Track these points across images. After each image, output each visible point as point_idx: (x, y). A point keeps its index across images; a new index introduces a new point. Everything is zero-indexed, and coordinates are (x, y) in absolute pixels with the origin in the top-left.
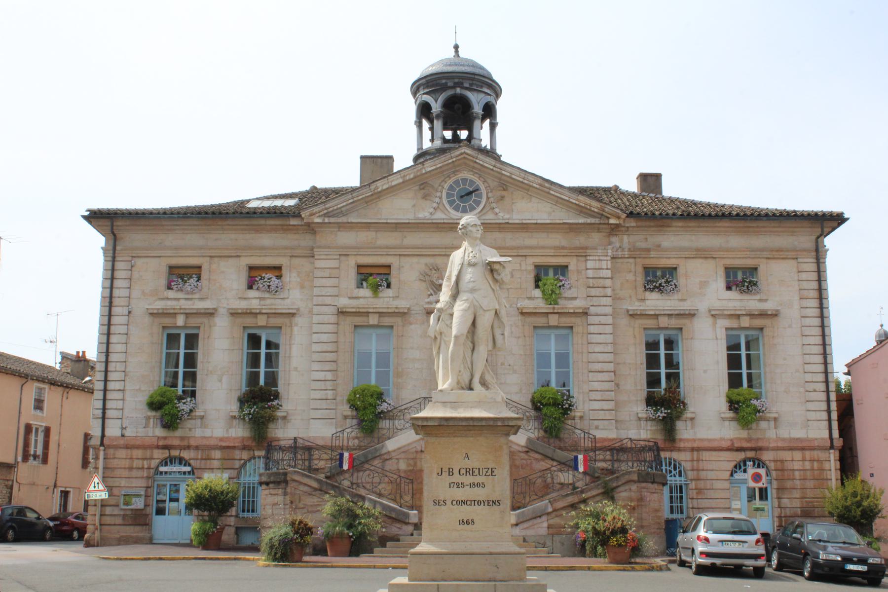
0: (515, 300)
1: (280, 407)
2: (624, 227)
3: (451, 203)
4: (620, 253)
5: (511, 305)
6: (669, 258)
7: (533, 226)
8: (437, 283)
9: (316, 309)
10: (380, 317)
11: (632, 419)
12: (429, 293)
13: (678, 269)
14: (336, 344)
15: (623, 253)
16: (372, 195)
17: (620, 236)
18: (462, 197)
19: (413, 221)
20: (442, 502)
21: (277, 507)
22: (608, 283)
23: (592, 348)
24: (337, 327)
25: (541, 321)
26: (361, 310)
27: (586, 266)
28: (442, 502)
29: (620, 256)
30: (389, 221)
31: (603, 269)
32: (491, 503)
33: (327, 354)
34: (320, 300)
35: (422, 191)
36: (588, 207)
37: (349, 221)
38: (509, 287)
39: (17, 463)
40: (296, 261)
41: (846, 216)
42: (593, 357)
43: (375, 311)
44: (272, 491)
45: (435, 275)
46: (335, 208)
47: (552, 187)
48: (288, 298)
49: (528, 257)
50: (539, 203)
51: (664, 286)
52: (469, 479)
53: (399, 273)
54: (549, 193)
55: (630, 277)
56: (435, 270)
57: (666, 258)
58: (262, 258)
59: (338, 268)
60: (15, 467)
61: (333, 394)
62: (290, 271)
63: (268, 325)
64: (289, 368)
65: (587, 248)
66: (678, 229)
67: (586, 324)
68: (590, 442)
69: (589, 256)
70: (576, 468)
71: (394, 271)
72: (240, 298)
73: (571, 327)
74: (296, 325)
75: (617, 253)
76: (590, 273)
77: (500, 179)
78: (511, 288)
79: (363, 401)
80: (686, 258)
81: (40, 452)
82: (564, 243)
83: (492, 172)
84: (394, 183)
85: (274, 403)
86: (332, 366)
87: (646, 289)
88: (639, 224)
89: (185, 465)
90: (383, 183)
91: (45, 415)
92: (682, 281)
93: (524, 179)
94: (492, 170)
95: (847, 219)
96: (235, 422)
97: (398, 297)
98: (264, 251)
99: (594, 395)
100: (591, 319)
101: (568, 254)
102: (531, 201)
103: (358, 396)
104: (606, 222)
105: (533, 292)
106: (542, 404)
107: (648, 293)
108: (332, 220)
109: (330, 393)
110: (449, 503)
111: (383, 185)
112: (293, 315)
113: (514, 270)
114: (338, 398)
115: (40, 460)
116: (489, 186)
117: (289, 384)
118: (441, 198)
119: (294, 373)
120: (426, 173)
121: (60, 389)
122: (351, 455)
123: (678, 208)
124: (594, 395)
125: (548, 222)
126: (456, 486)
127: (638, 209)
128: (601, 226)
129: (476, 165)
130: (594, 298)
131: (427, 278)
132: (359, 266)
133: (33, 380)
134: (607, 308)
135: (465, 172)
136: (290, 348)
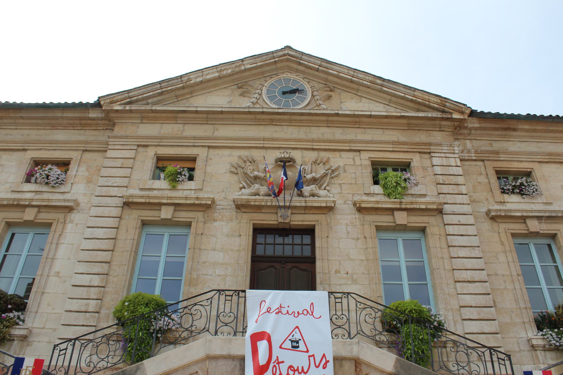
0: (350, 196)
1: (21, 323)
2: (466, 128)
3: (271, 98)
4: (466, 155)
5: (345, 201)
6: (521, 161)
8: (252, 175)
9: (96, 201)
10: (175, 210)
11: (522, 348)
12: (241, 185)
13: (533, 173)
14: (113, 241)
15: (470, 155)
16: (183, 88)
17: (462, 140)
18: (284, 93)
19: (227, 110)
22: (461, 180)
23: (454, 252)
24: (119, 222)
25: (385, 220)
26: (152, 201)
27: (432, 163)
29: (467, 158)
30: (198, 109)
31: (453, 166)
33: (99, 252)
34: (104, 191)
35: (240, 91)
36: (427, 103)
37: (154, 108)
38: (342, 182)
40: (87, 155)
42: (458, 263)
43: (169, 201)
45: (249, 168)
46: (140, 97)
47: (385, 83)
48: (69, 192)
49: (361, 152)
50: (370, 103)
51: (525, 186)
53: (206, 165)
54: (381, 91)
55: (482, 179)
56: (250, 162)
57: (518, 161)
58: (51, 152)
59: (134, 158)
61: (97, 305)
62: (79, 165)
63: (37, 221)
64: (49, 273)
65: (430, 144)
66: (525, 134)
67: (442, 225)
69: (434, 152)
71: (199, 164)
72: (12, 191)
73: (423, 230)
74: (71, 222)
75: (463, 155)
76: (438, 170)
77: (327, 80)
78: (344, 183)
79: (132, 312)
80: (539, 162)
82: (403, 139)
83: (317, 73)
84: (209, 77)
85: (11, 315)
86: (104, 268)
87: (503, 192)
88: (483, 125)
90: (196, 76)
92: (541, 185)
93: (353, 77)
94: (317, 70)
97: (201, 190)
98: (55, 145)
99: (467, 313)
100: (448, 219)
101: (409, 150)
102: (361, 101)
103: (126, 304)
104: (449, 116)
105: (372, 187)
106: (400, 321)
107: (506, 196)
108: (134, 107)
109: (93, 303)
111: (196, 78)
112: (70, 209)
113: (345, 165)
114: (103, 311)
116: (314, 87)
117: (43, 293)
118: (260, 95)
119: (53, 280)
120: (245, 70)
124: (467, 313)
125: (384, 114)
128: (444, 123)
129: (300, 68)
130: (447, 195)
131: (240, 170)
132: (159, 159)
134: (465, 206)
135: (288, 74)
136: (57, 249)
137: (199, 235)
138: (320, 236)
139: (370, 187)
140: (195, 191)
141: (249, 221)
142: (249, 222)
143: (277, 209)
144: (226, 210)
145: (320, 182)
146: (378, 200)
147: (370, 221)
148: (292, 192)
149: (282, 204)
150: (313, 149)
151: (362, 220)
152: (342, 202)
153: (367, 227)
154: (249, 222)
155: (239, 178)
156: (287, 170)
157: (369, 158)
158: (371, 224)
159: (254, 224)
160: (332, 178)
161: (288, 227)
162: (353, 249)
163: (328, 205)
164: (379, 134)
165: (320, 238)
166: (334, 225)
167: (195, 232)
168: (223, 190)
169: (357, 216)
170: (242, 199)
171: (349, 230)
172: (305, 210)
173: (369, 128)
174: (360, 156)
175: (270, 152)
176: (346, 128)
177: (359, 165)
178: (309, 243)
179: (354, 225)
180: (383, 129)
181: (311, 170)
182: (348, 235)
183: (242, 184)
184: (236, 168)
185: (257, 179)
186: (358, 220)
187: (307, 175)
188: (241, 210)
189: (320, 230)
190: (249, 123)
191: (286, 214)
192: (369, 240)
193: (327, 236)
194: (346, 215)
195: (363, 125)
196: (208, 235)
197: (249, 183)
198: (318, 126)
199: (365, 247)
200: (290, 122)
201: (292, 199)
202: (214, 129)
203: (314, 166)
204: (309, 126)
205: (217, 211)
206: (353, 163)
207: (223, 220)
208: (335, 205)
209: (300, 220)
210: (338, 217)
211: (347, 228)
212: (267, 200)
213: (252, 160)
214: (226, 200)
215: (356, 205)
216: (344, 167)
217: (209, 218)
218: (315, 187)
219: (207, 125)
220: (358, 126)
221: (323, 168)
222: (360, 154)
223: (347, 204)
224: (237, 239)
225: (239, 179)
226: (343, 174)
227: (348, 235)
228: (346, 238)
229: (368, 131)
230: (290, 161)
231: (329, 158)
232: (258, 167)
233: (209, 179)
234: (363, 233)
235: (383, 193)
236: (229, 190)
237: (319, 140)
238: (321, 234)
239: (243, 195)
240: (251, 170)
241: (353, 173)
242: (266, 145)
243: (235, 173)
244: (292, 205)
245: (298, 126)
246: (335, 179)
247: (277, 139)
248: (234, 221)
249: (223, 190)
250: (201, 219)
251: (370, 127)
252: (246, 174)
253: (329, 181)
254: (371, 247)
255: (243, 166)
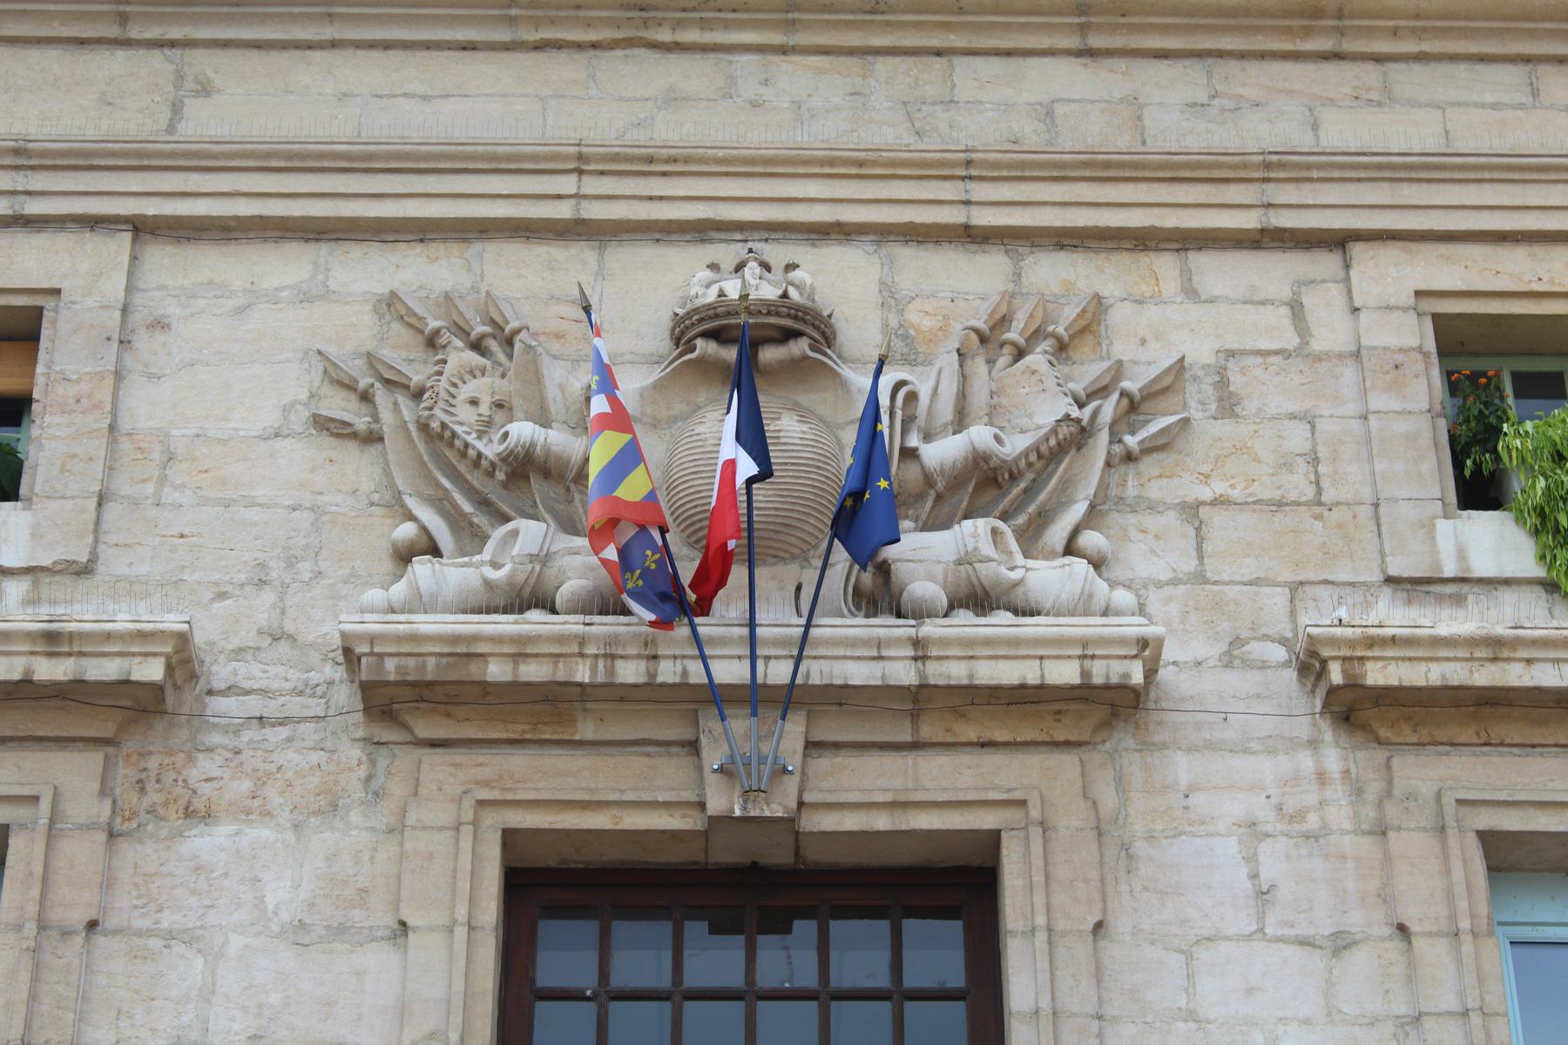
0: (1276, 600)
5: (1237, 642)
12: (407, 531)
38: (1206, 494)
49: (1357, 250)
53: (119, 376)
56: (477, 346)
78: (1220, 502)
97: (84, 571)
105: (1444, 527)
113: (1231, 354)
131: (392, 412)
137: (66, 933)
138: (1041, 920)
139: (1429, 527)
140: (36, 584)
141: (469, 815)
142: (475, 823)
143: (696, 711)
144: (284, 732)
145: (1029, 493)
146: (1501, 630)
147: (1439, 796)
148: (810, 578)
149: (731, 671)
150: (972, 237)
151: (1374, 789)
152: (1205, 649)
153: (1412, 844)
154: (475, 823)
155: (387, 471)
156: (767, 402)
157: (1419, 294)
158: (1450, 822)
159: (510, 837)
160: (1129, 458)
161: (780, 856)
162: (1307, 1021)
163: (1101, 672)
164: (1495, 106)
165: (1041, 937)
166: (1151, 838)
167: (32, 909)
168: (263, 566)
169: (1333, 760)
170: (414, 638)
171: (1266, 875)
172: (915, 716)
173: (1421, 58)
174: (1347, 280)
175: (628, 259)
176: (1234, 65)
177: (1340, 356)
178: (956, 978)
179: (1307, 836)
180: (1527, 59)
181: (962, 397)
182: (1261, 917)
183: (411, 517)
184: (366, 397)
185: (535, 482)
186: (1338, 793)
187: (928, 437)
188: (406, 727)
189: (1039, 878)
190: (461, 35)
191: (767, 748)
192: (1431, 951)
193: (1099, 926)
194: (1247, 751)
195: (1370, 32)
196: (140, 934)
197: (467, 507)
198: (1008, 53)
199: (1402, 1009)
200: (790, 25)
201: (814, 632)
202: (180, 78)
203: (979, 366)
204: (938, 53)
205: (215, 738)
206: (1290, 340)
207: (267, 814)
208: (1150, 673)
209: (879, 797)
210: (1182, 767)
211: (1251, 859)
212: (611, 640)
213: (487, 329)
214: (283, 648)
215: (1322, 673)
216: (1222, 372)
217: (153, 797)
218: (995, 532)
219: (121, 53)
220: (1324, 44)
221: (1050, 383)
222: (1347, 267)
223: (1249, 665)
224: (379, 960)
225: (392, 485)
226: (1209, 431)
227: (1261, 917)
228: (1249, 937)
229: (1407, 79)
230: (788, 335)
231: (1097, 307)
232: (538, 379)
233: (150, 488)
234: (1386, 898)
235: (1540, 572)
236: (306, 569)
237: (1021, 165)
238: (1048, 911)
239: (419, 603)
240: (484, 409)
241: (1293, 417)
242: (596, 211)
243: (354, 435)
244: (815, 680)
245: (851, 52)
246: (1148, 466)
247: (687, 160)
248: (355, 817)
249: (263, 566)
250: (85, 804)
251: (1428, 46)
252: (439, 438)
253: (1103, 486)
254: (1449, 1002)
255: (417, 376)
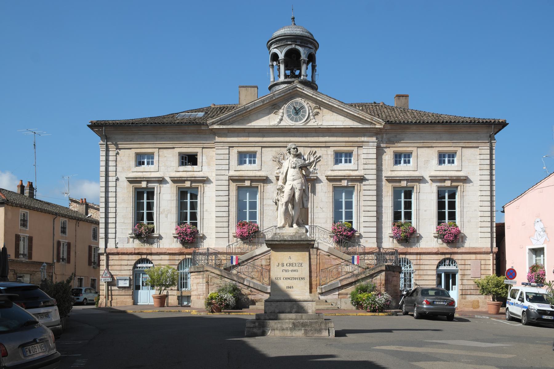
7: (335, 130)
20: (279, 279)
21: (199, 284)
28: (279, 279)
32: (301, 279)
39: (54, 263)
41: (507, 122)
44: (197, 276)
52: (291, 268)
60: (53, 265)
68: (362, 250)
70: (353, 263)
81: (65, 256)
89: (150, 263)
91: (67, 236)
95: (508, 124)
96: (175, 239)
104: (374, 127)
110: (282, 279)
115: (66, 261)
121: (74, 221)
122: (237, 257)
123: (415, 117)
126: (285, 271)
127: (392, 119)
133: (60, 216)
152: (320, 175)
186: (326, 183)
252: (279, 162)
